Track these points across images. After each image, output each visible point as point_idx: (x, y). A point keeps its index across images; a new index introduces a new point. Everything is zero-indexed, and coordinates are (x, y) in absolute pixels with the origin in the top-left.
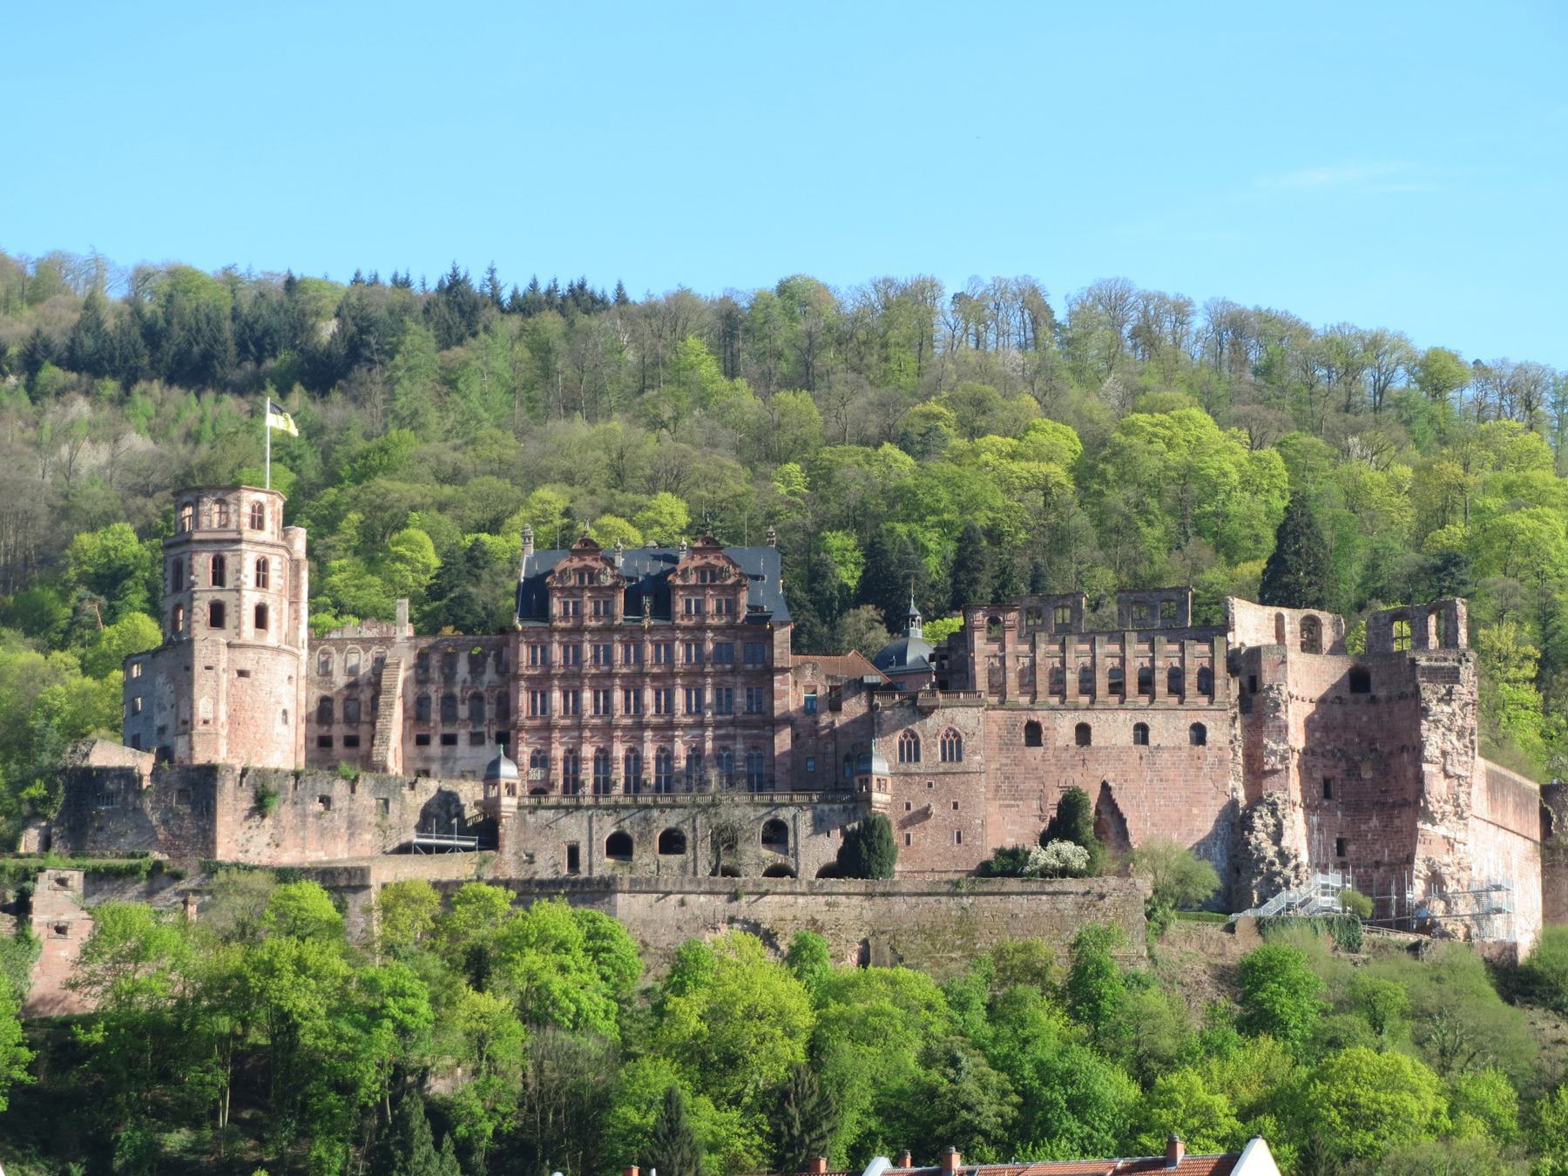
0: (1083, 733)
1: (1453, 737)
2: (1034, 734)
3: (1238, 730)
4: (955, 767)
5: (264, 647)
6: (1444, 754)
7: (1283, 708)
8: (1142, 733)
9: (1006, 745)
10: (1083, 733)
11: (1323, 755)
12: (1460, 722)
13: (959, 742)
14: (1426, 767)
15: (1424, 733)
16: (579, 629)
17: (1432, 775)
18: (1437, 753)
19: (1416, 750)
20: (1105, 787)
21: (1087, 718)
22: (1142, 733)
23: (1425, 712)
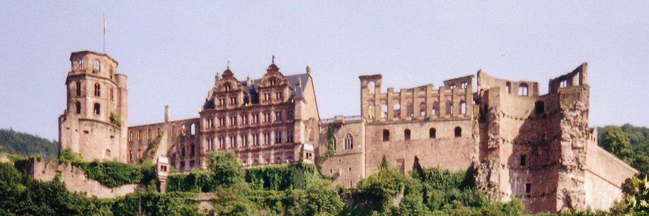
0: (407, 133)
1: (577, 129)
2: (386, 134)
3: (477, 129)
4: (351, 151)
5: (97, 121)
6: (572, 137)
7: (497, 117)
8: (433, 133)
9: (375, 141)
10: (407, 133)
11: (521, 144)
12: (580, 120)
13: (352, 140)
14: (562, 143)
15: (562, 126)
16: (225, 111)
17: (566, 147)
18: (569, 136)
19: (558, 136)
20: (416, 159)
21: (410, 127)
22: (433, 133)
23: (562, 116)
